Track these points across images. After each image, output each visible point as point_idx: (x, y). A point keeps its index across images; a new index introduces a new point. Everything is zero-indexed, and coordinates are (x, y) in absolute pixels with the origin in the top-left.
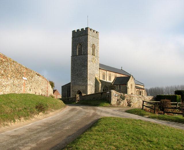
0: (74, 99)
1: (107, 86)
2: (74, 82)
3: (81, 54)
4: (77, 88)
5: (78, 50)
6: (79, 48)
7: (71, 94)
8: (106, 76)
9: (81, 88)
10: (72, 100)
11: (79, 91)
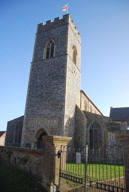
0: (35, 159)
1: (100, 123)
2: (32, 111)
3: (52, 56)
4: (38, 124)
5: (45, 51)
6: (48, 49)
7: (22, 136)
8: (87, 107)
9: (47, 124)
10: (25, 161)
11: (42, 129)
